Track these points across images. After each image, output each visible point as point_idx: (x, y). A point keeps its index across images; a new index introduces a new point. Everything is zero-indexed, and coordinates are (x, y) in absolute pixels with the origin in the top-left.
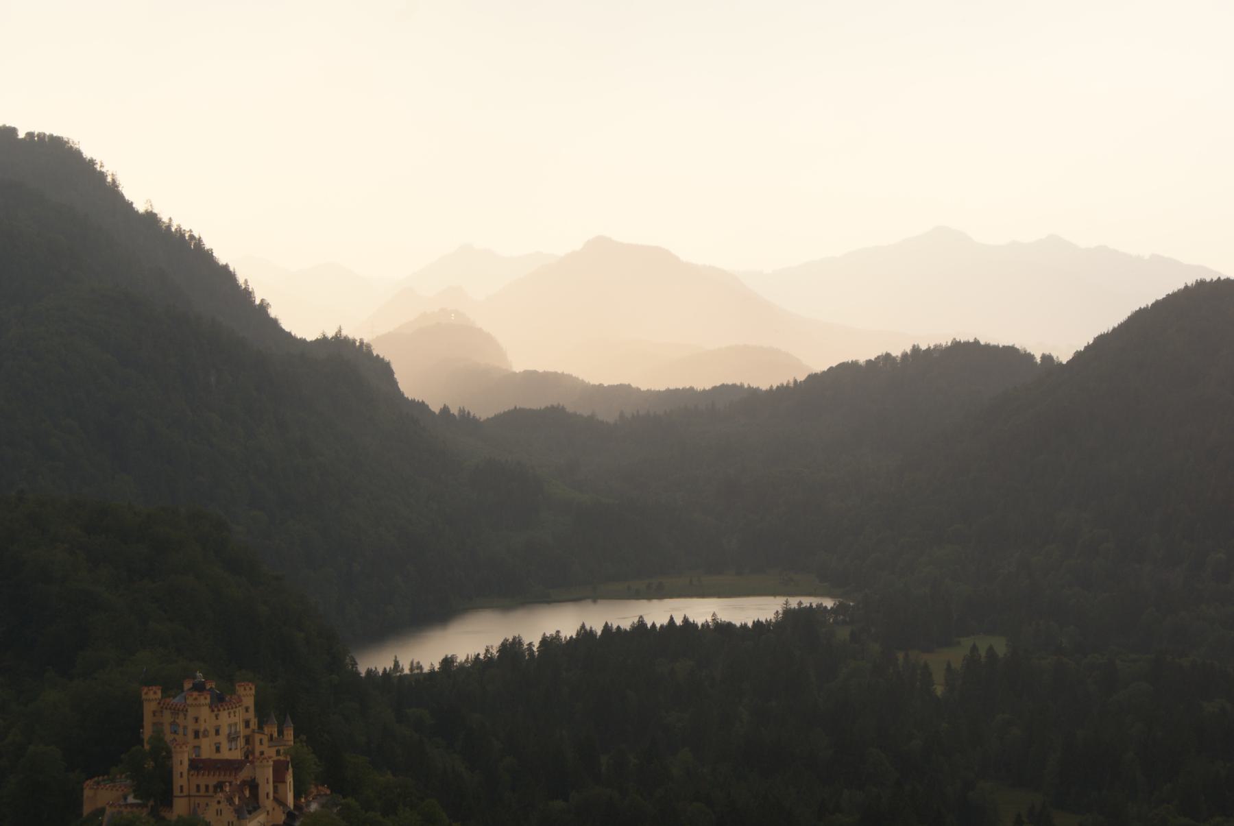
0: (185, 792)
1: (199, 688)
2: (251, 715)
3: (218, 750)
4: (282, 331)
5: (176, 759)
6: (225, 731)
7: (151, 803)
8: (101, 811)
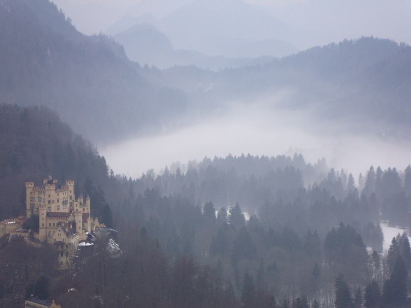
0: (45, 226)
1: (50, 182)
2: (72, 194)
3: (58, 209)
4: (76, 32)
5: (41, 213)
6: (61, 201)
7: (30, 231)
8: (8, 235)
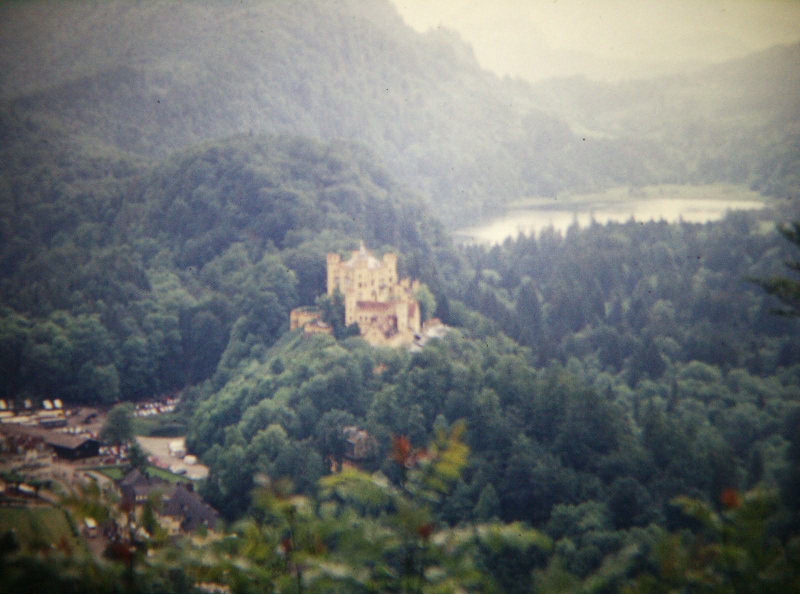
6: (377, 284)
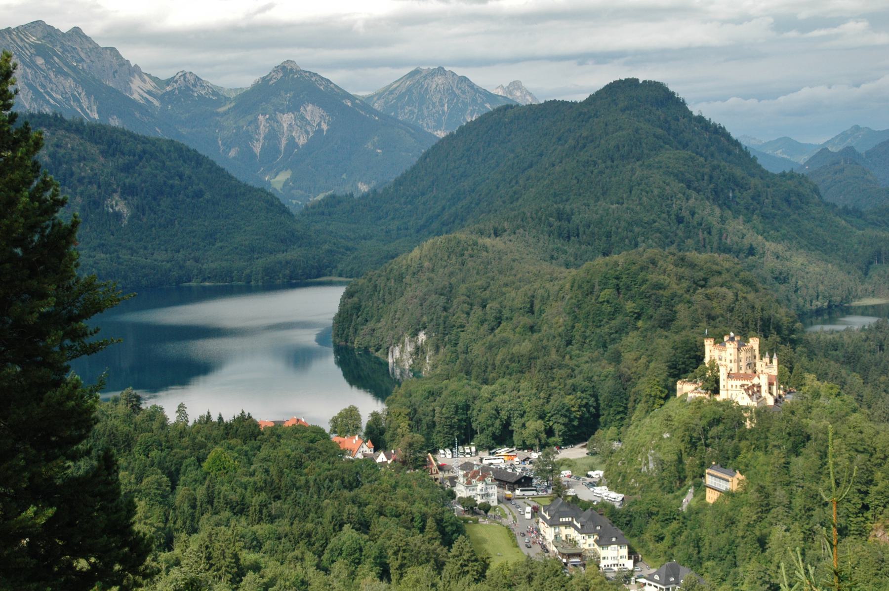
1: (732, 339)
